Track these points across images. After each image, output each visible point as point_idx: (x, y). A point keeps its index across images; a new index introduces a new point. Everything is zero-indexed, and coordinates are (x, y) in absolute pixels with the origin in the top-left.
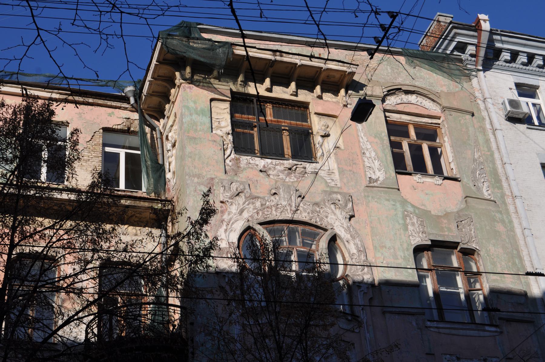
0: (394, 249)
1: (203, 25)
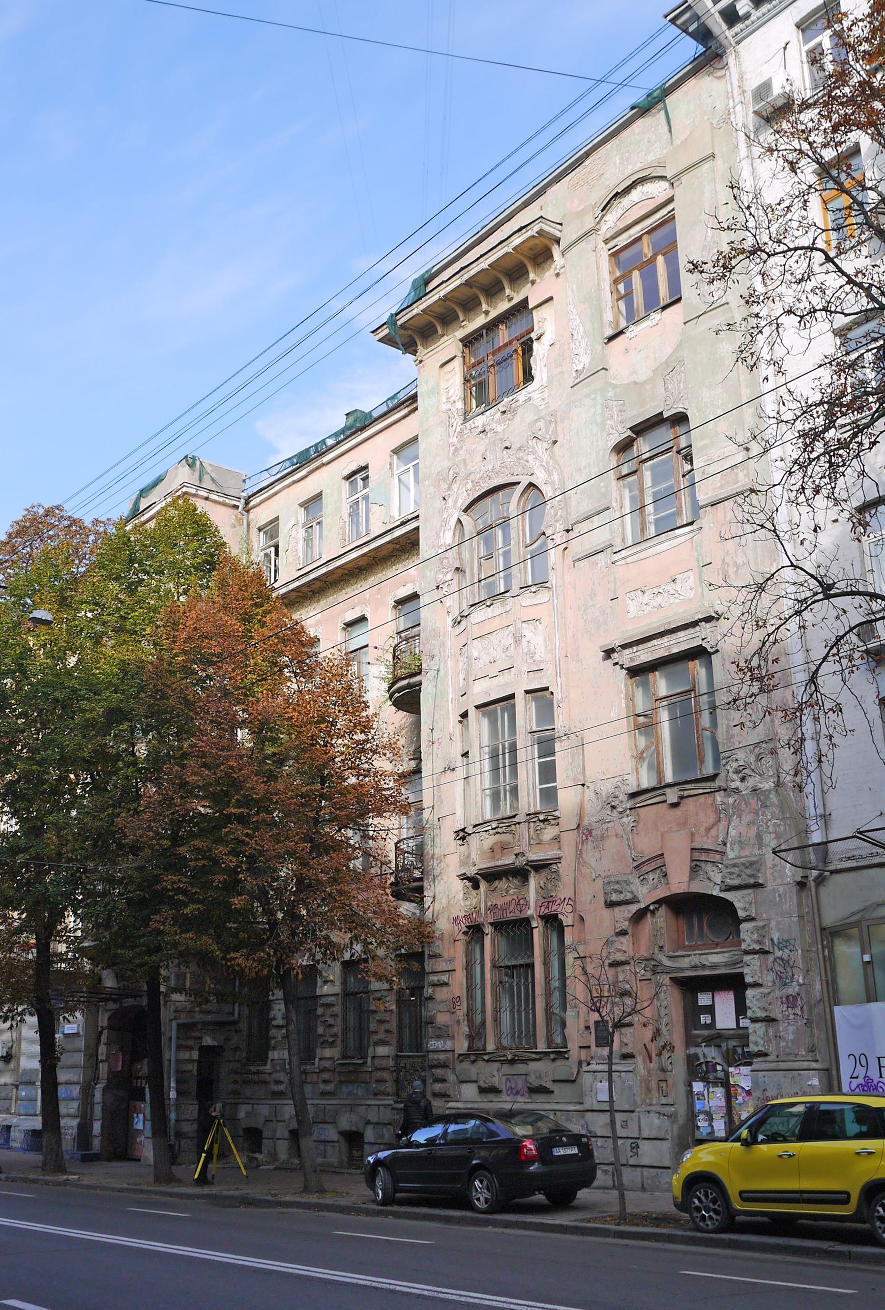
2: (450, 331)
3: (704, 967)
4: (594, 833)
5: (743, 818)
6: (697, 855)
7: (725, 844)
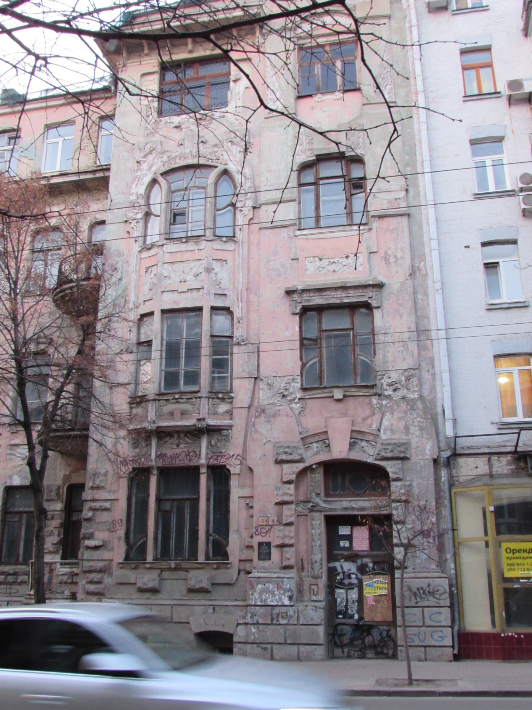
3: (353, 509)
4: (267, 411)
5: (395, 414)
6: (355, 435)
7: (379, 430)
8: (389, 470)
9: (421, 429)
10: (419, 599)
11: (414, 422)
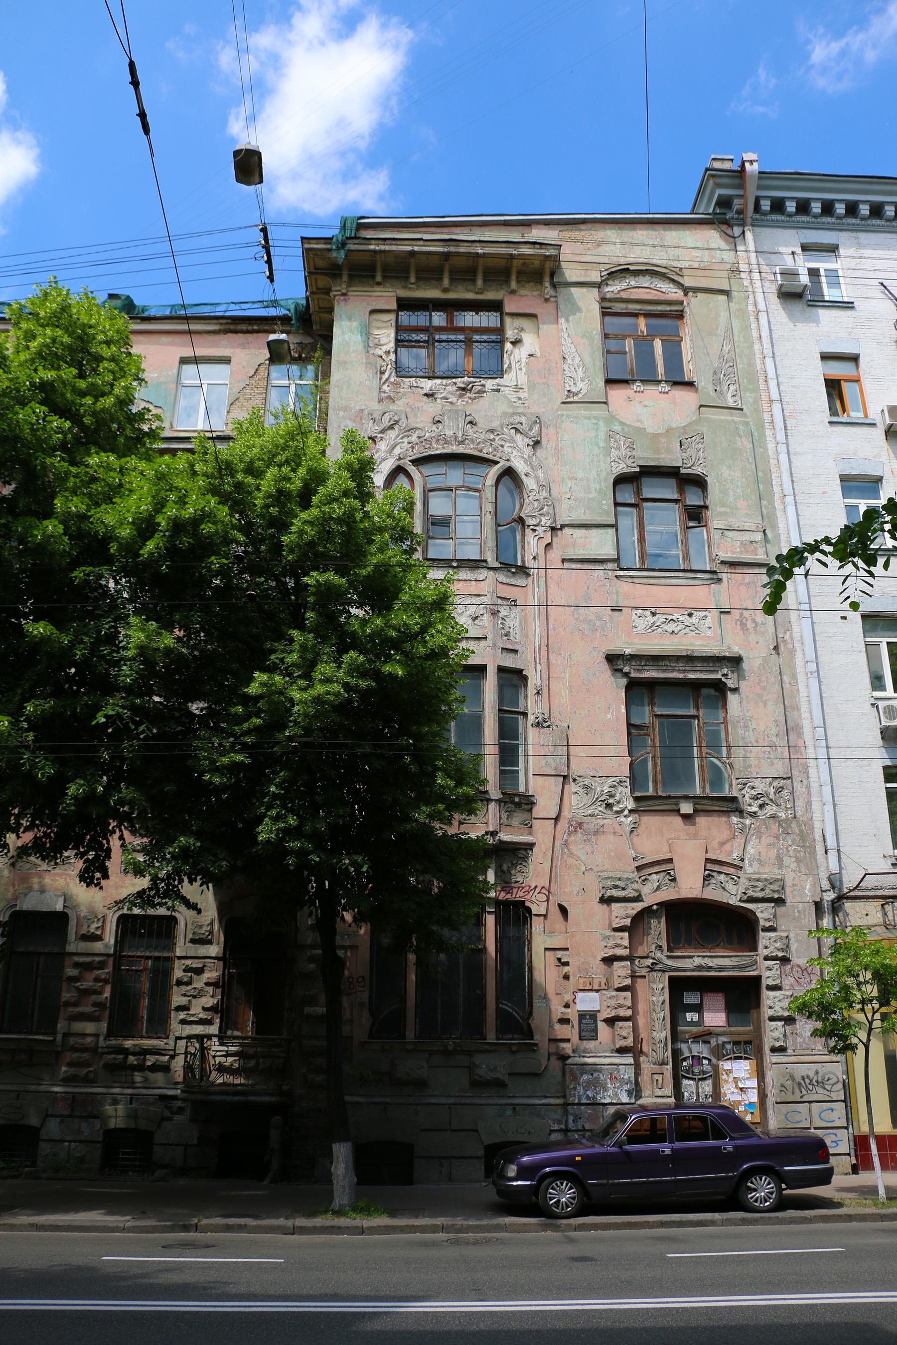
0: (588, 480)
1: (368, 218)
2: (387, 285)
4: (585, 826)
5: (763, 838)
6: (709, 866)
7: (742, 860)
8: (759, 915)
9: (798, 861)
10: (804, 1092)
11: (788, 851)
